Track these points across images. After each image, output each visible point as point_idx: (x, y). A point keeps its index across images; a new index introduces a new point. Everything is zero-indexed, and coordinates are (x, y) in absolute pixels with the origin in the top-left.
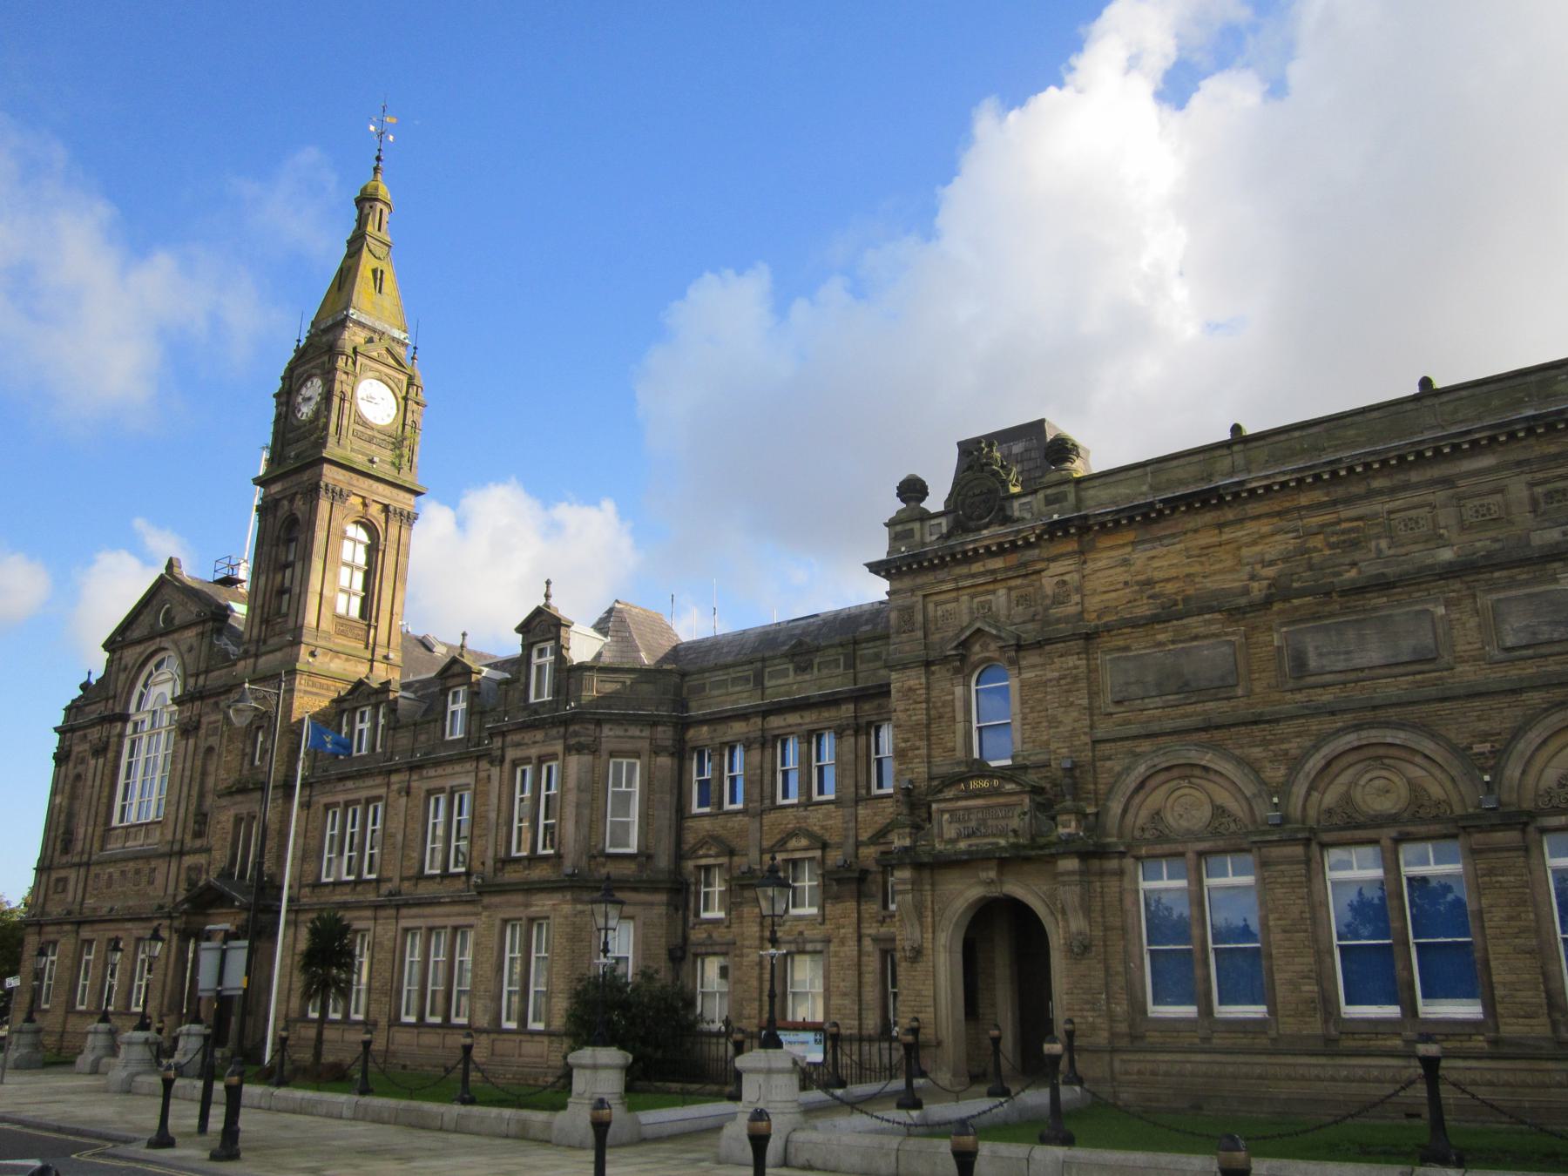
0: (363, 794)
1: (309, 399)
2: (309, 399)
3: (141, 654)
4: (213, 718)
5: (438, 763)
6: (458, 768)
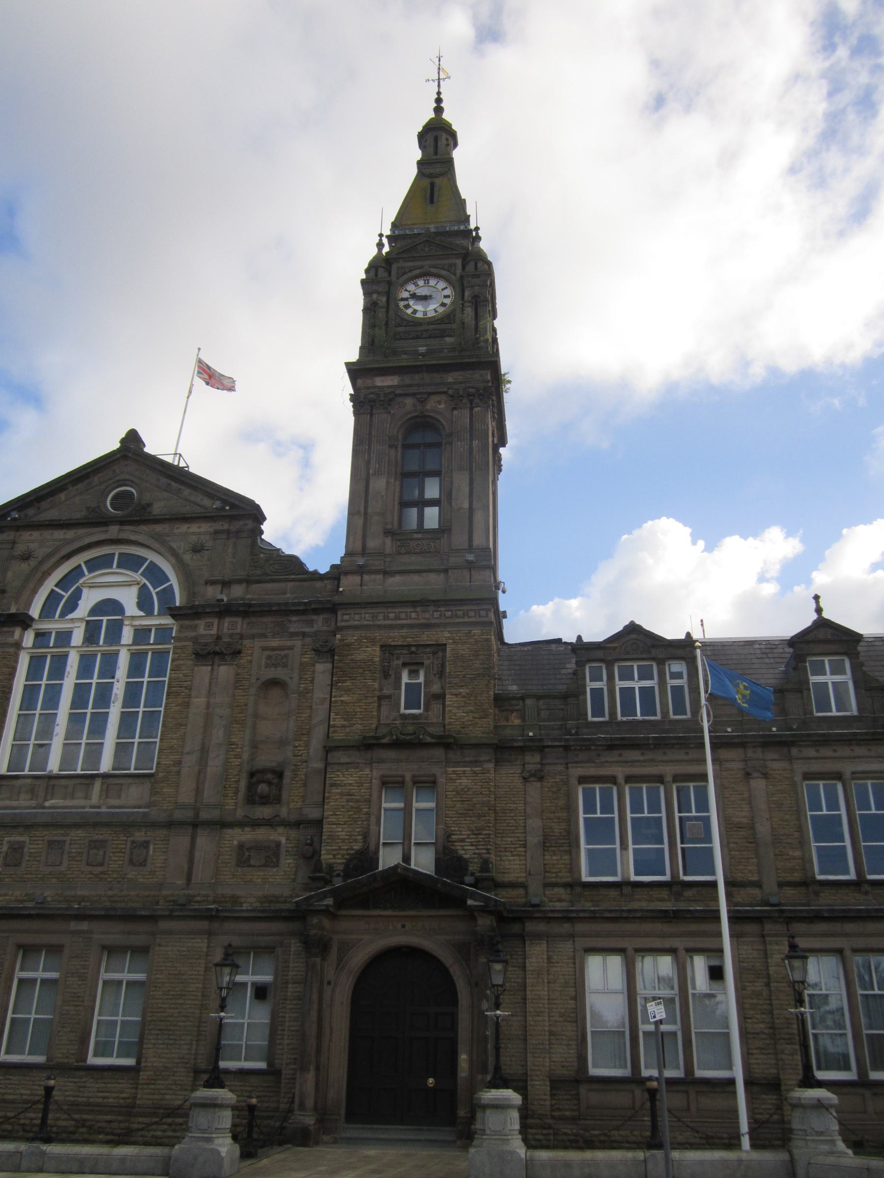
0: (669, 770)
1: (425, 298)
2: (425, 298)
3: (72, 541)
4: (275, 643)
5: (825, 741)
6: (861, 751)
